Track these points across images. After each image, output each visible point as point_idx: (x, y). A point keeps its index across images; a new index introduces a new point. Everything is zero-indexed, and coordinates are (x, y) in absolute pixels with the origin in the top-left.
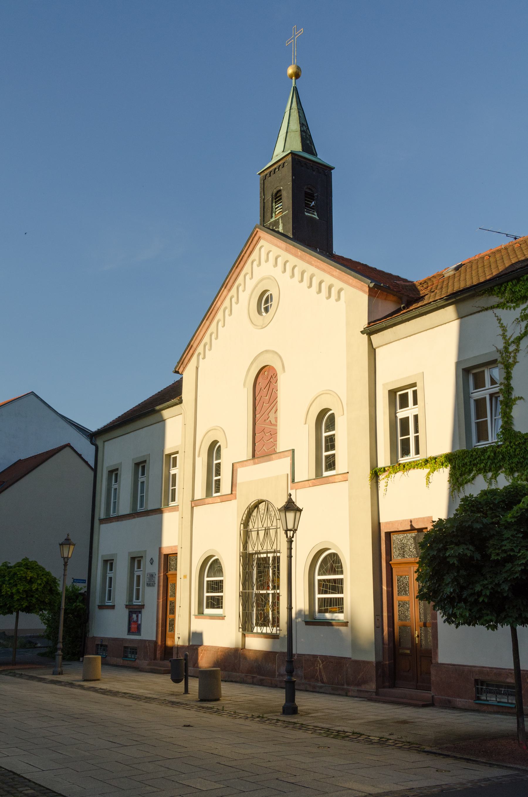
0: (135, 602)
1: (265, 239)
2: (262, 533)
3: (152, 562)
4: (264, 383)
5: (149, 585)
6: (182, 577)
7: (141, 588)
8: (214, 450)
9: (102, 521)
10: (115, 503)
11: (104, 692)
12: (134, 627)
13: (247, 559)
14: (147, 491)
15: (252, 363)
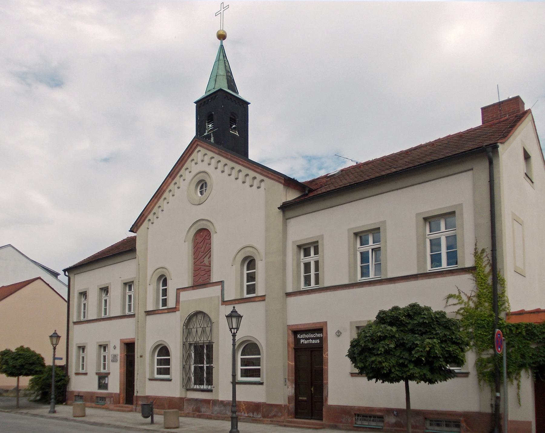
0: (102, 371)
1: (201, 146)
2: (200, 330)
3: (115, 348)
4: (202, 238)
5: (113, 361)
6: (139, 357)
7: (106, 363)
8: (164, 280)
9: (75, 323)
10: (84, 313)
11: (94, 424)
12: (102, 385)
13: (186, 346)
14: (110, 305)
15: (191, 227)
